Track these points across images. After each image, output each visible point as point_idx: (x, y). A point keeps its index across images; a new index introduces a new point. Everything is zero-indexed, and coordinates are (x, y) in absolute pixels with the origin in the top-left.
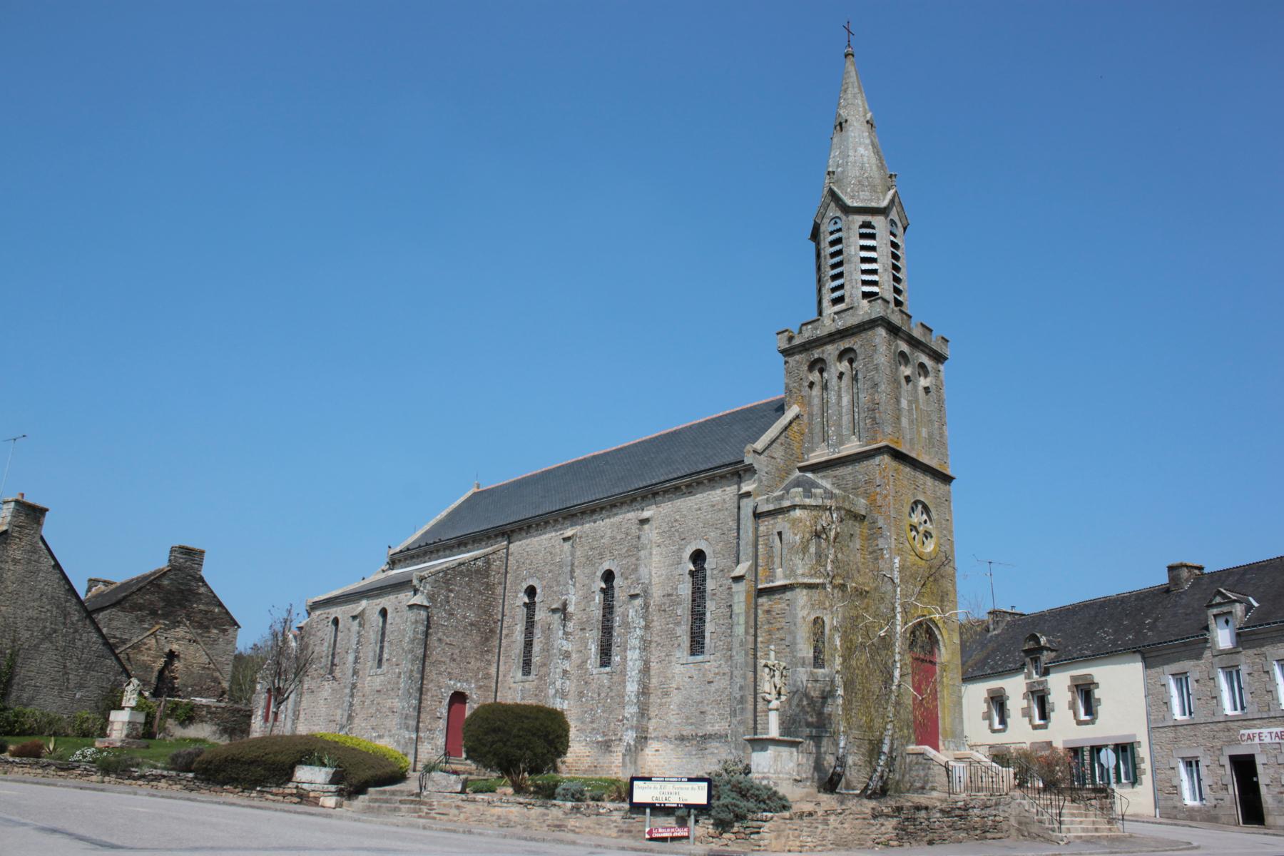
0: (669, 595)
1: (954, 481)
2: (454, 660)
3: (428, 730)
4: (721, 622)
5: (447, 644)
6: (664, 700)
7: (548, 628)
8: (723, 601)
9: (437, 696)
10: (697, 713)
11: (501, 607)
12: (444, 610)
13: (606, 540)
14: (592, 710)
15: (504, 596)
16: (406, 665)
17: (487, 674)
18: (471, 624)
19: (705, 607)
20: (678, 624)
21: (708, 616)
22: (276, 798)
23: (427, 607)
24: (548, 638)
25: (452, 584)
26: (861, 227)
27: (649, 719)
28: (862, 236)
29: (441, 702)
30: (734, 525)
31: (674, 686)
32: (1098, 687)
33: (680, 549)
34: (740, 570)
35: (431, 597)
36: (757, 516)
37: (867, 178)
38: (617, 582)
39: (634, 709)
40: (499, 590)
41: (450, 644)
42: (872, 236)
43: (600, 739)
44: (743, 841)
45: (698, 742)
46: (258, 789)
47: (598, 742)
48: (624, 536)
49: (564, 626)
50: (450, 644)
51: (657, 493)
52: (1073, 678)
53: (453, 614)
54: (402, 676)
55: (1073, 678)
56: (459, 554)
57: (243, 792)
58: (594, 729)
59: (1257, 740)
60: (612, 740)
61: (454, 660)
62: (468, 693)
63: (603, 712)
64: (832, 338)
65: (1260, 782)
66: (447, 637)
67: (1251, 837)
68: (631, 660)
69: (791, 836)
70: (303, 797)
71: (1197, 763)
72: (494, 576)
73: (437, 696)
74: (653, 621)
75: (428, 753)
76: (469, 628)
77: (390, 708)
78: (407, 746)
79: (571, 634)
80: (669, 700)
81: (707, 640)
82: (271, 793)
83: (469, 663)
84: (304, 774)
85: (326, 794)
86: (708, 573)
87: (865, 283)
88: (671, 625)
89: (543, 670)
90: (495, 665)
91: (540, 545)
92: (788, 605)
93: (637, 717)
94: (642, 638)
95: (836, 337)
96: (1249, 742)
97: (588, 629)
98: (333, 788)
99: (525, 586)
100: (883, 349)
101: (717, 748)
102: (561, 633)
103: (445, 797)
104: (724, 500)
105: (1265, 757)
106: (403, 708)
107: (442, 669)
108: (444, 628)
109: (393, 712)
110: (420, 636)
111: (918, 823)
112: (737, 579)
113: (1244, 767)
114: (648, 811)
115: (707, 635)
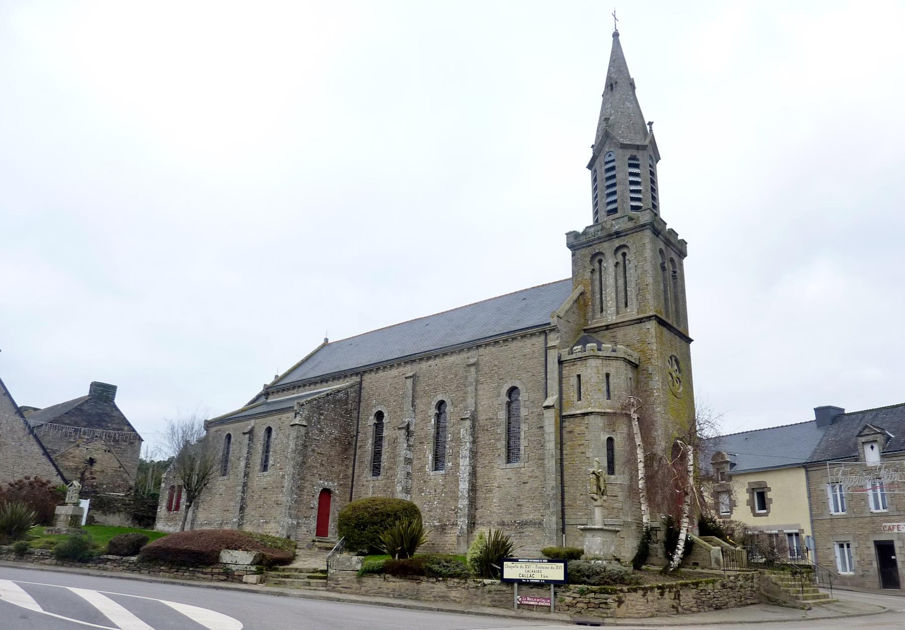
0: (490, 419)
1: (692, 342)
2: (323, 465)
3: (304, 517)
4: (533, 439)
5: (318, 453)
6: (487, 495)
7: (395, 440)
8: (534, 424)
9: (311, 492)
10: (515, 506)
11: (356, 426)
12: (317, 428)
13: (439, 379)
14: (429, 502)
15: (358, 418)
16: (289, 469)
17: (346, 475)
18: (335, 439)
19: (519, 428)
20: (499, 440)
21: (522, 433)
22: (206, 576)
23: (305, 426)
24: (394, 448)
25: (322, 410)
26: (629, 159)
27: (476, 509)
28: (631, 165)
29: (313, 496)
30: (543, 371)
31: (496, 485)
32: (770, 491)
33: (499, 386)
34: (550, 401)
35: (308, 419)
36: (560, 362)
37: (633, 124)
38: (449, 409)
39: (466, 502)
40: (355, 414)
41: (320, 454)
42: (637, 166)
43: (437, 524)
44: (593, 609)
45: (516, 527)
46: (191, 569)
47: (435, 526)
48: (453, 376)
49: (408, 440)
50: (320, 454)
51: (480, 346)
52: (749, 483)
53: (322, 431)
54: (286, 477)
55: (749, 483)
56: (321, 388)
57: (177, 571)
58: (431, 516)
59: (896, 530)
60: (446, 525)
61: (323, 465)
62: (332, 489)
63: (439, 503)
64: (589, 244)
65: (897, 560)
66: (319, 448)
67: (888, 599)
68: (462, 466)
69: (629, 605)
70: (229, 575)
71: (848, 546)
72: (351, 403)
73: (311, 492)
74: (478, 437)
75: (304, 534)
76: (334, 441)
77: (275, 501)
78: (290, 530)
79: (412, 446)
80: (492, 495)
81: (522, 452)
82: (203, 573)
83: (333, 467)
84: (227, 557)
85: (248, 573)
86: (522, 403)
87: (633, 199)
88: (492, 441)
89: (390, 472)
90: (351, 469)
91: (386, 382)
92: (587, 428)
93: (468, 508)
94: (471, 451)
95: (613, 237)
96: (890, 532)
97: (425, 443)
98: (254, 568)
99: (375, 411)
100: (648, 246)
101: (532, 532)
102: (405, 445)
103: (348, 574)
104: (534, 351)
105: (901, 542)
106: (287, 501)
107: (315, 472)
108: (317, 441)
109: (278, 504)
110: (300, 448)
111: (707, 593)
112: (547, 407)
113: (885, 550)
114: (516, 585)
115: (522, 448)
